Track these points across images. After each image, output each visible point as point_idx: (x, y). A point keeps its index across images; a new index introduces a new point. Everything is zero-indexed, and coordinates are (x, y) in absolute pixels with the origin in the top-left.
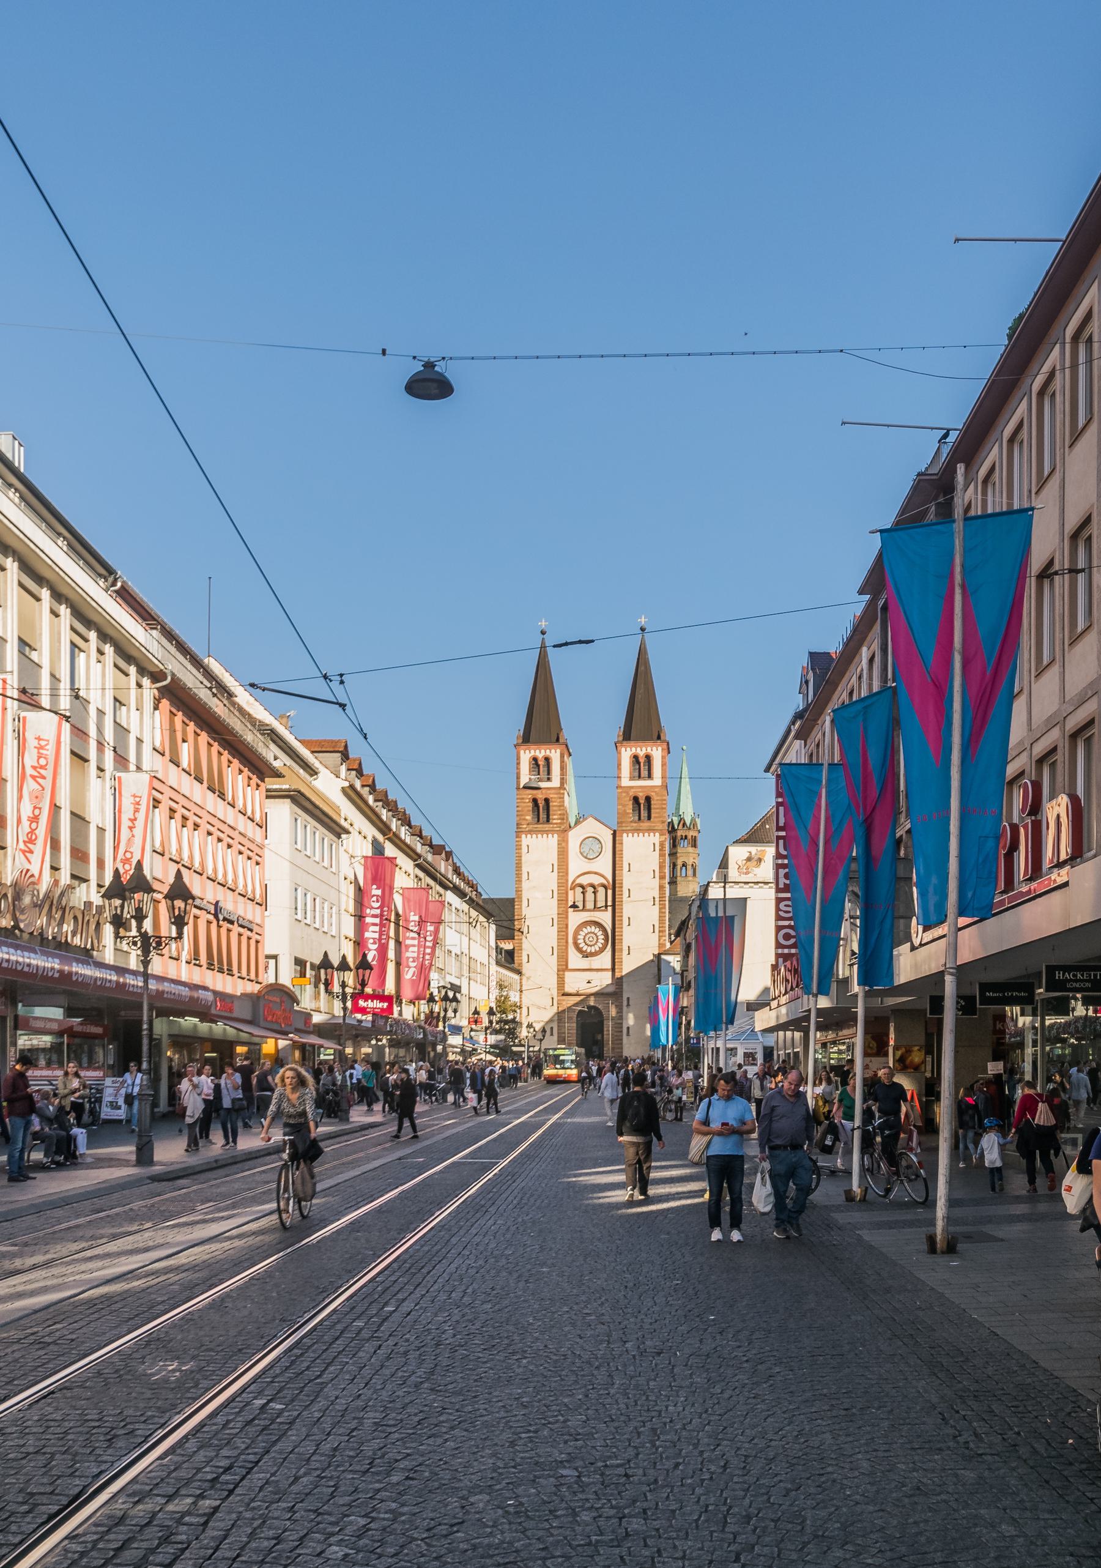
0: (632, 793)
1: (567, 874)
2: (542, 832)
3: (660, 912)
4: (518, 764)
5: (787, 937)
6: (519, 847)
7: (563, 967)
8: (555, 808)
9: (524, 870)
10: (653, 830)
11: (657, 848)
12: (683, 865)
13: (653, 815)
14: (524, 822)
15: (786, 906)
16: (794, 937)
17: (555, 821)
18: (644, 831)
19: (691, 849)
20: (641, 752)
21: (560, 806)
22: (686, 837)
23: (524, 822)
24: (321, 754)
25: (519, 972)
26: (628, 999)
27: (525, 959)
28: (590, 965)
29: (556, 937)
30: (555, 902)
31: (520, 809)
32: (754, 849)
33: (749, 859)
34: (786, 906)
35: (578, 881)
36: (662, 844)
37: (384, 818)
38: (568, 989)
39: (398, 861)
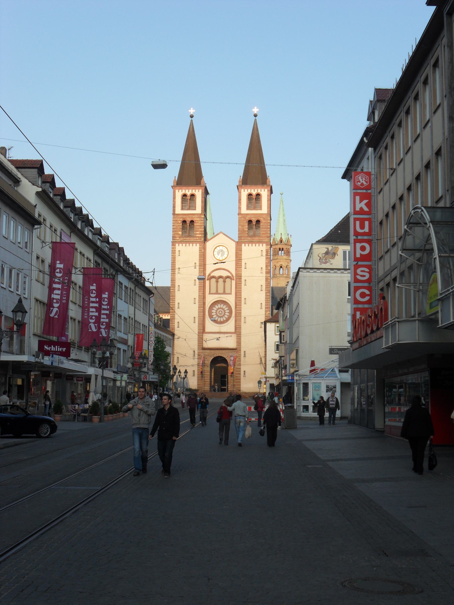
0: (248, 218)
2: (189, 242)
4: (174, 198)
5: (363, 295)
6: (174, 252)
7: (202, 330)
8: (197, 227)
9: (177, 266)
11: (264, 253)
12: (281, 267)
14: (177, 236)
15: (362, 271)
16: (368, 295)
17: (197, 235)
18: (256, 243)
19: (285, 257)
20: (254, 192)
21: (201, 226)
22: (283, 249)
23: (177, 236)
24: (23, 170)
29: (197, 311)
31: (175, 227)
32: (330, 247)
33: (327, 253)
34: (362, 271)
35: (212, 275)
36: (267, 251)
37: (72, 220)
38: (206, 345)
39: (77, 246)
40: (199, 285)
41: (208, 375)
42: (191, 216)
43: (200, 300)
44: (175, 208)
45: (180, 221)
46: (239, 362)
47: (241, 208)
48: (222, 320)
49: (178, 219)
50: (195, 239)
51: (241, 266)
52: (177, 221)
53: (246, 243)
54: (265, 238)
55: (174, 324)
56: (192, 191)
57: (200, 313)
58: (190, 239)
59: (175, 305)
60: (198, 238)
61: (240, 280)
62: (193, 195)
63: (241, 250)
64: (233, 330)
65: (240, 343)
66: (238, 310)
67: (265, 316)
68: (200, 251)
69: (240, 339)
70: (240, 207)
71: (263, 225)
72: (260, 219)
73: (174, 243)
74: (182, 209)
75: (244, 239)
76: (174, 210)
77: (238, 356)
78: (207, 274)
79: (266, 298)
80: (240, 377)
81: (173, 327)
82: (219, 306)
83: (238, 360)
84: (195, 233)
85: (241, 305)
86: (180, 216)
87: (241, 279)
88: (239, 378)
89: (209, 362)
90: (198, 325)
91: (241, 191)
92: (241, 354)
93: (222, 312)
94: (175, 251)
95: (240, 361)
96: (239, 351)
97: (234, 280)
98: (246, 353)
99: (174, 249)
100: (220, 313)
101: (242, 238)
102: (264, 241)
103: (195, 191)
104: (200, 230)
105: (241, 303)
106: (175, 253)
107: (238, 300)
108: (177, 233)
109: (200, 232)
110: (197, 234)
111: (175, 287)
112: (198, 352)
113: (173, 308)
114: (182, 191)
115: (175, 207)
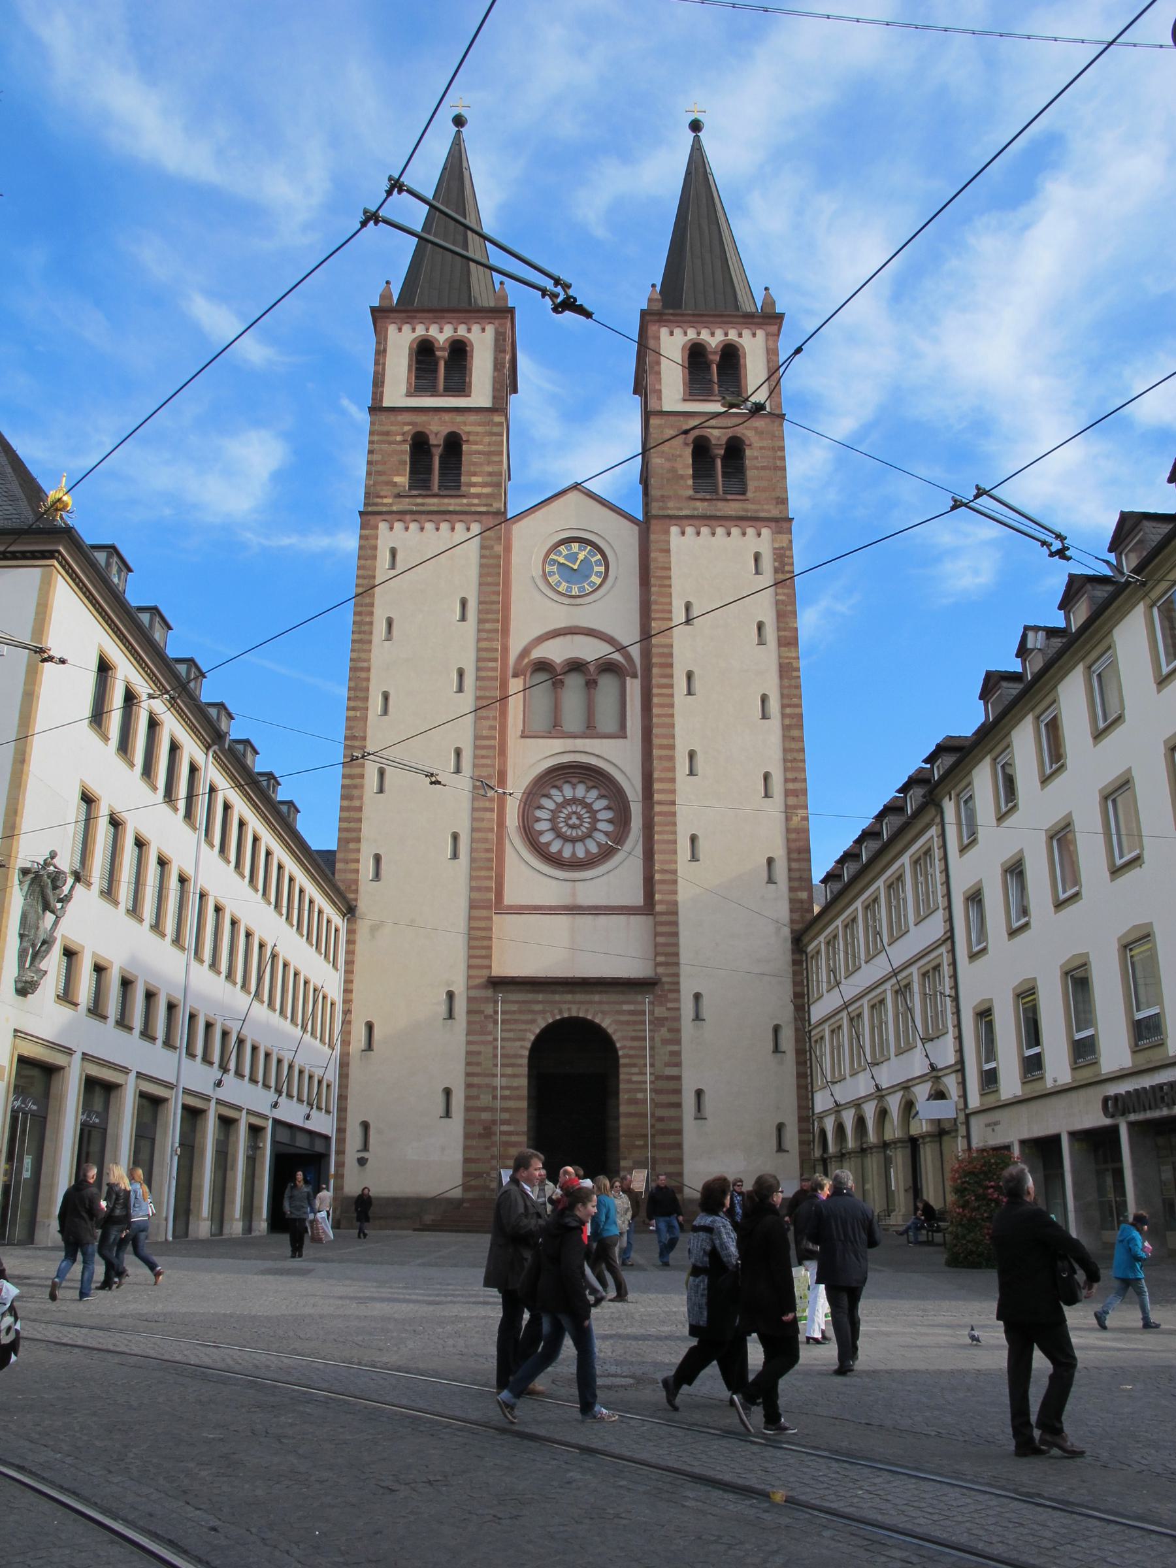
1: (506, 631)
3: (786, 737)
6: (367, 551)
8: (475, 459)
10: (754, 520)
13: (751, 485)
17: (473, 490)
20: (713, 339)
21: (489, 454)
25: (349, 911)
26: (697, 997)
27: (366, 868)
28: (574, 895)
30: (467, 700)
31: (376, 457)
35: (537, 654)
38: (506, 964)
40: (478, 688)
41: (518, 1110)
42: (447, 417)
43: (483, 757)
44: (382, 386)
45: (403, 434)
46: (675, 1048)
47: (660, 390)
48: (581, 854)
49: (393, 428)
50: (462, 505)
51: (670, 612)
52: (387, 433)
53: (685, 522)
54: (765, 507)
55: (353, 866)
56: (456, 330)
57: (477, 815)
58: (444, 504)
59: (362, 776)
60: (476, 501)
61: (667, 671)
62: (460, 351)
63: (668, 551)
64: (638, 900)
65: (677, 954)
66: (660, 803)
67: (788, 830)
68: (487, 552)
69: (676, 934)
70: (657, 387)
71: (757, 458)
72: (743, 434)
73: (369, 516)
74: (409, 394)
75: (677, 505)
76: (378, 394)
77: (666, 1019)
78: (516, 646)
79: (785, 750)
80: (679, 1119)
81: (351, 876)
82: (568, 791)
83: (668, 1036)
84: (463, 479)
85: (673, 780)
86: (402, 418)
87: (671, 666)
88: (673, 1125)
89: (522, 1047)
90: (471, 869)
91: (659, 332)
92: (678, 1009)
93: (579, 818)
94: (375, 548)
95: (678, 1042)
96: (670, 991)
97: (635, 676)
98: (705, 1001)
99: (372, 542)
100: (571, 822)
101: (671, 504)
102: (762, 514)
103: (469, 330)
104: (490, 469)
105: (673, 769)
106: (374, 557)
107: (661, 758)
108: (384, 478)
109: (488, 479)
110: (474, 485)
111: (366, 699)
112: (470, 1000)
113: (355, 792)
114: (414, 330)
115: (383, 382)
